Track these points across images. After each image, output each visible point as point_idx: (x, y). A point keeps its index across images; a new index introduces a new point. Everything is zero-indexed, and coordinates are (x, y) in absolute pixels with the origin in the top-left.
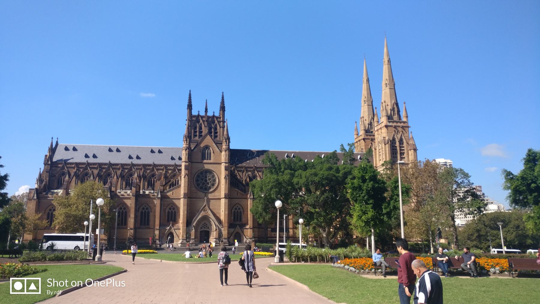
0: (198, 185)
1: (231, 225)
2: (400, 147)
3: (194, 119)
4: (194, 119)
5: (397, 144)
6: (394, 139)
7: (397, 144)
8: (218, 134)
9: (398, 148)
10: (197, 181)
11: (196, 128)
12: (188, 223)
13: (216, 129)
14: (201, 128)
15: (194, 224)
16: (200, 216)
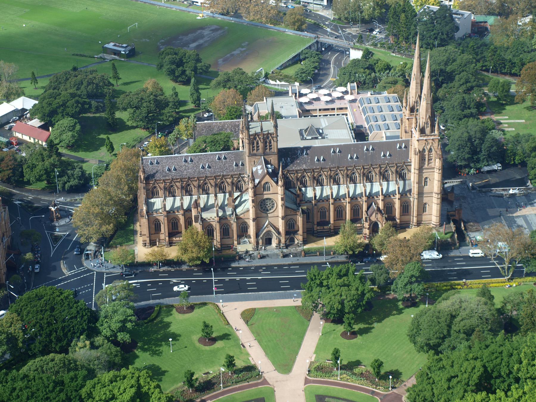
0: (262, 208)
1: (287, 233)
2: (429, 155)
3: (251, 137)
4: (251, 137)
5: (427, 153)
6: (424, 150)
7: (427, 153)
8: (272, 147)
9: (427, 156)
10: (261, 205)
11: (253, 144)
12: (257, 235)
13: (270, 142)
14: (257, 143)
15: (261, 236)
16: (265, 231)
